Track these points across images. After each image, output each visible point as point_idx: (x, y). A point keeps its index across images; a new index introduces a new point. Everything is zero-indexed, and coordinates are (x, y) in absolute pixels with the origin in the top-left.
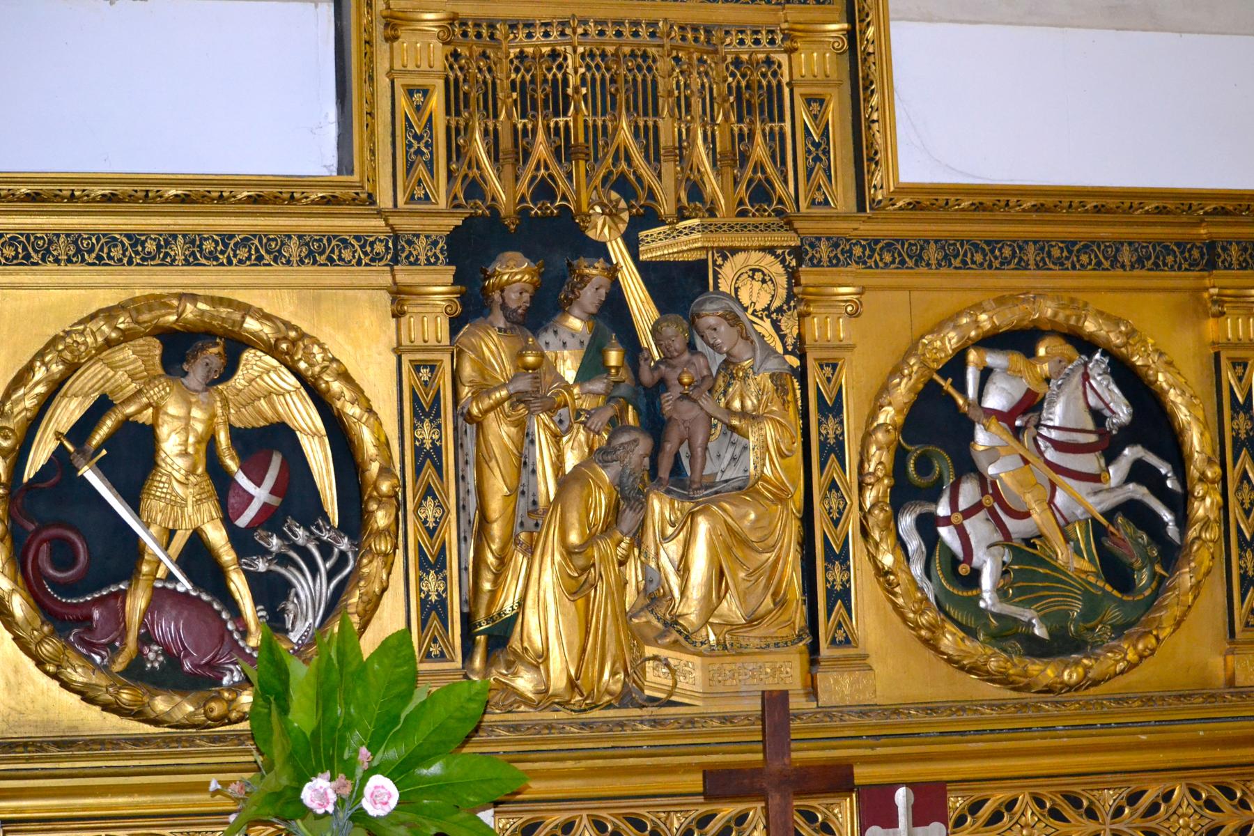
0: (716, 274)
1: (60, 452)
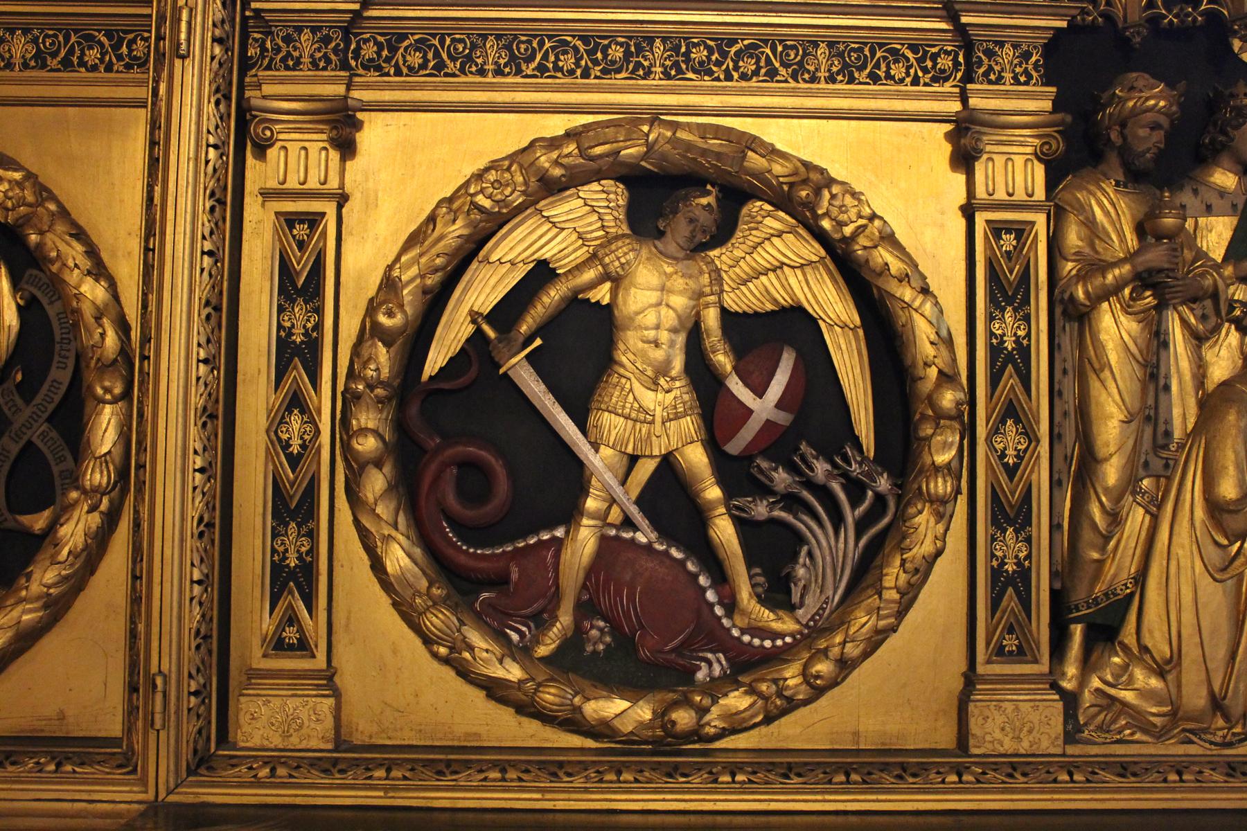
1: (478, 337)
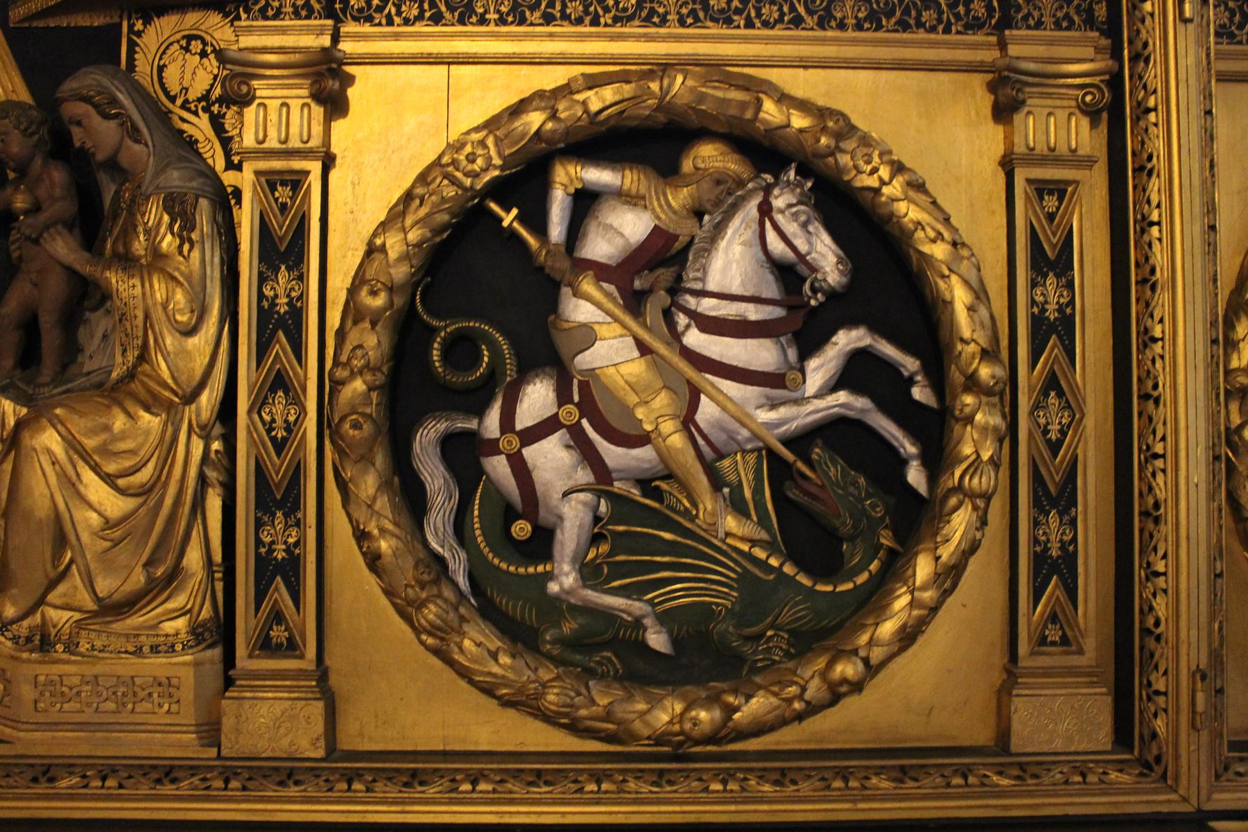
0: (132, 46)
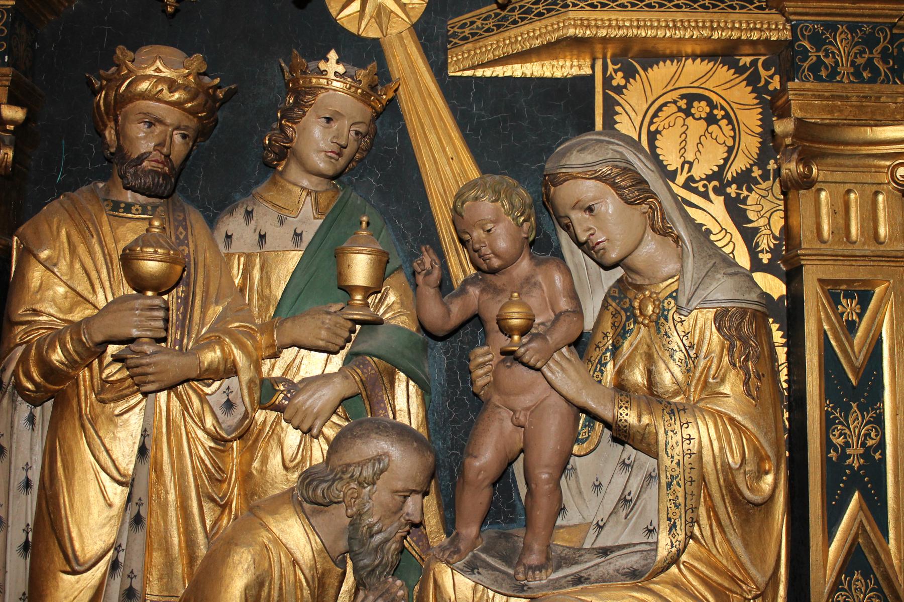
0: (610, 107)
